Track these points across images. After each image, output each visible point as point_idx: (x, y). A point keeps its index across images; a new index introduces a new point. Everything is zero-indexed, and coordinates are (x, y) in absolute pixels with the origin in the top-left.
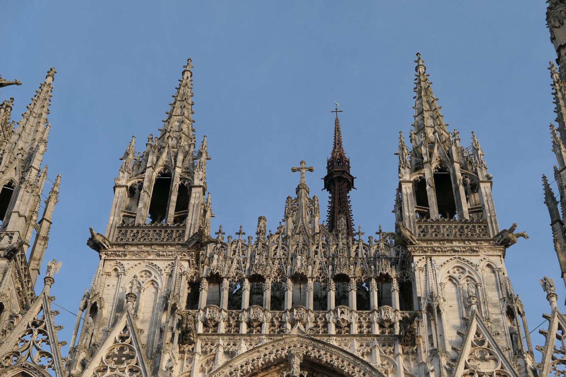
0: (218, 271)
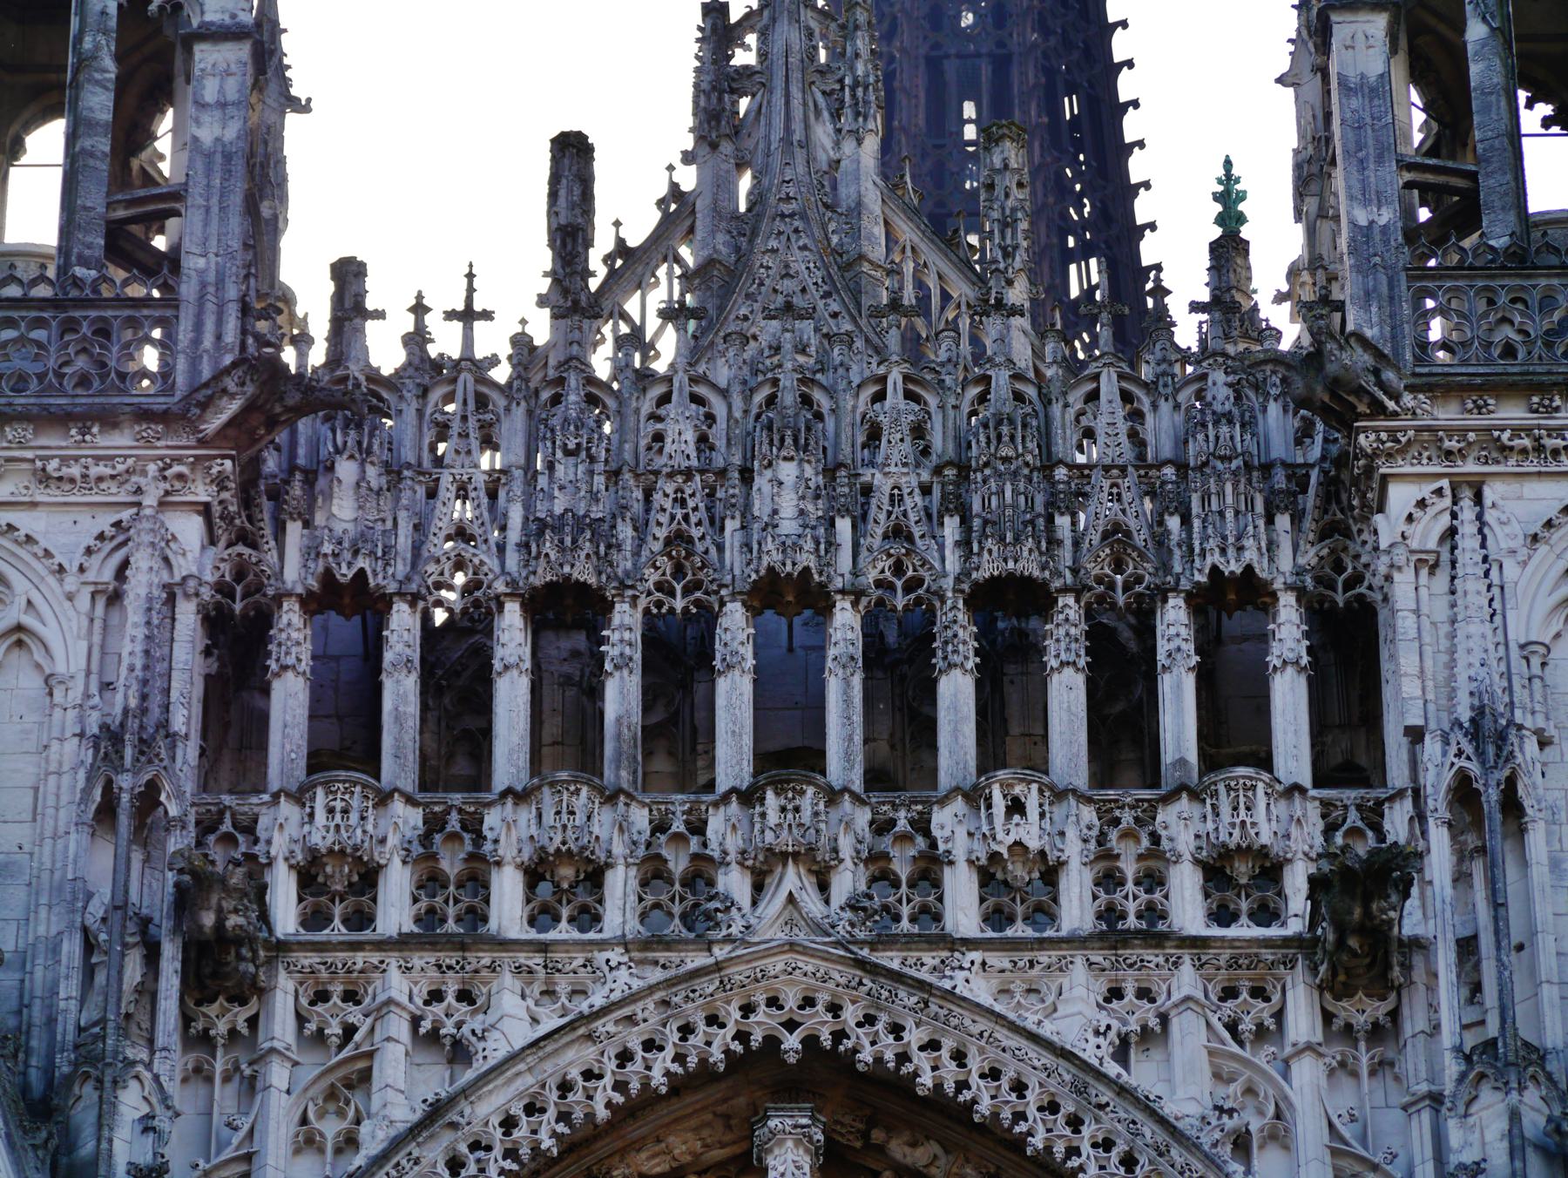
0: (362, 562)
